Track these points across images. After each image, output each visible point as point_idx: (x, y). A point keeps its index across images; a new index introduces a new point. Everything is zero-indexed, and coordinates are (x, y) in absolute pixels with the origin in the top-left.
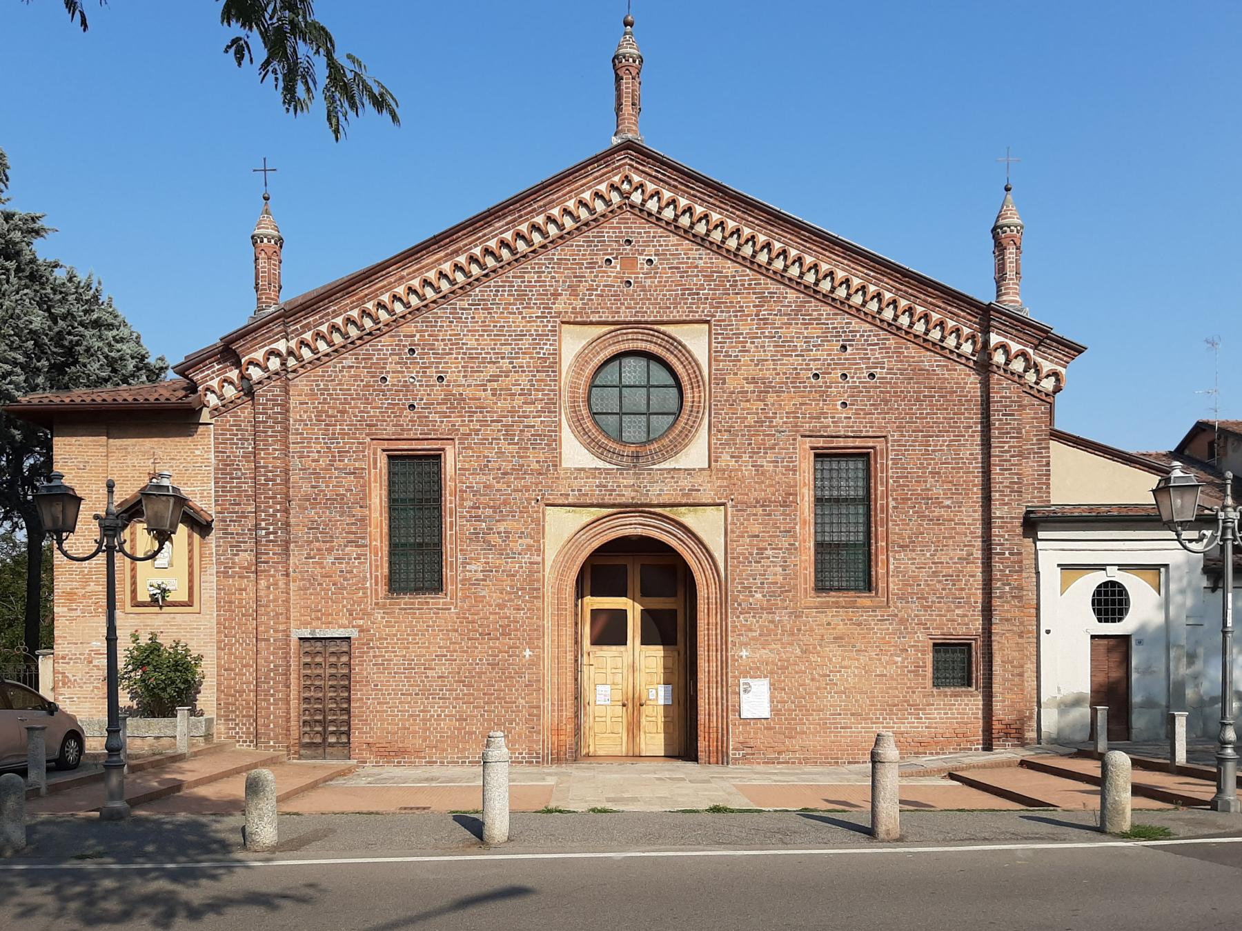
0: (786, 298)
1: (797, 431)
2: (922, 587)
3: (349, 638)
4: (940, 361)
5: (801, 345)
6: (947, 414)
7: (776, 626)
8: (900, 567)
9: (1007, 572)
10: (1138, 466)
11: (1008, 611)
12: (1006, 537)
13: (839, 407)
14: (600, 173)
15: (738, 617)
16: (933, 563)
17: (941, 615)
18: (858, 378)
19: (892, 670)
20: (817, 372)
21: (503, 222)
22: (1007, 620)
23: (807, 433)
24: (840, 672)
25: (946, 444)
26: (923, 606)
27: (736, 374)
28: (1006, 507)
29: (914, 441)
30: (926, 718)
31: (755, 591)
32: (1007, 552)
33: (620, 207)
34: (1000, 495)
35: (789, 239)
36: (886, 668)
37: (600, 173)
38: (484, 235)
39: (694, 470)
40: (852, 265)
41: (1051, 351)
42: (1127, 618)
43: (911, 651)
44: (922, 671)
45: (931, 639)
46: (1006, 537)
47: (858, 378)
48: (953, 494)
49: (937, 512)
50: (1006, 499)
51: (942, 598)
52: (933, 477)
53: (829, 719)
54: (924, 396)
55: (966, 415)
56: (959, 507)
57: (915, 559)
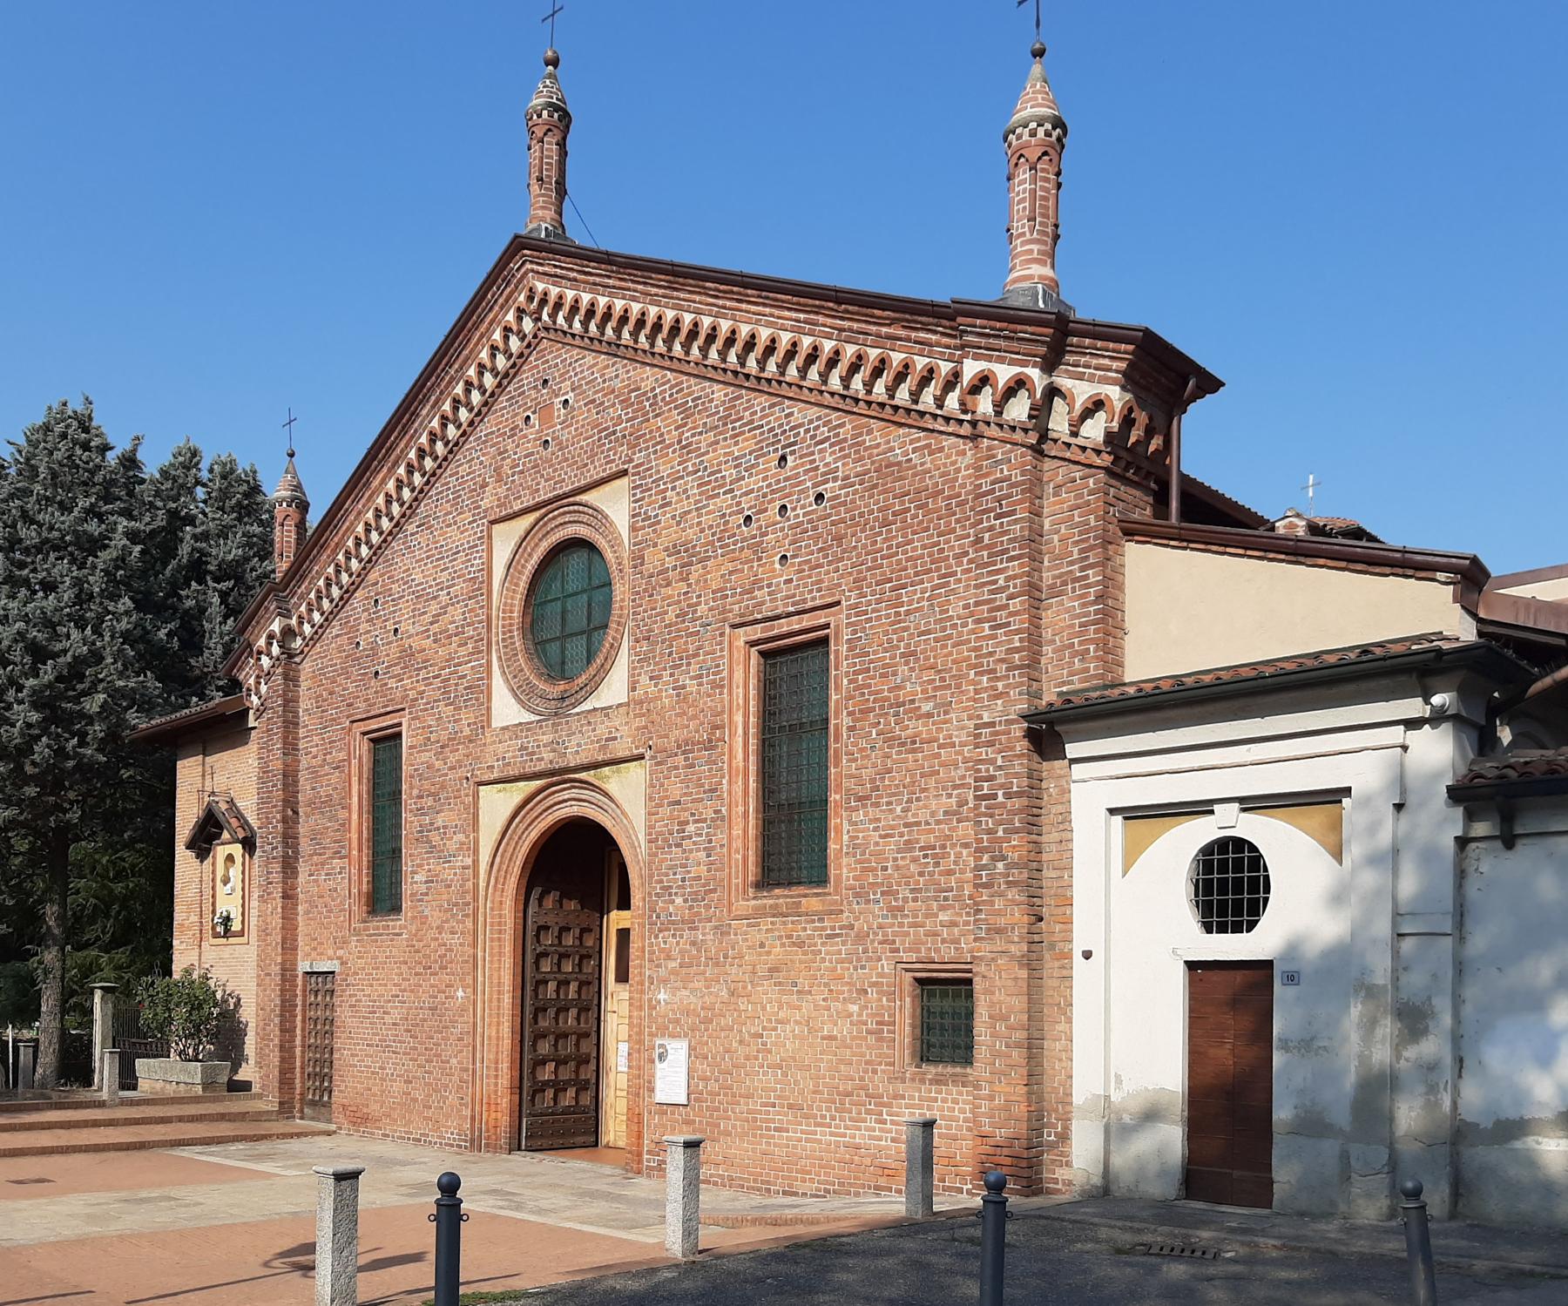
0: (711, 401)
1: (724, 620)
2: (890, 871)
3: (333, 972)
4: (919, 439)
5: (729, 473)
6: (929, 537)
7: (699, 951)
8: (858, 838)
9: (1000, 833)
10: (1321, 561)
11: (999, 913)
12: (999, 762)
13: (777, 566)
14: (504, 296)
15: (656, 937)
16: (906, 825)
17: (915, 925)
18: (803, 507)
19: (844, 1029)
20: (749, 513)
21: (428, 407)
22: (999, 931)
23: (738, 620)
24: (775, 1029)
25: (927, 595)
26: (891, 909)
27: (655, 545)
28: (1000, 702)
29: (878, 602)
30: (893, 1122)
31: (676, 894)
32: (1000, 793)
33: (535, 336)
34: (990, 680)
35: (700, 303)
36: (836, 1025)
37: (504, 296)
38: (416, 431)
39: (611, 707)
40: (776, 312)
41: (1087, 358)
42: (1265, 920)
43: (873, 994)
44: (889, 1032)
45: (907, 970)
46: (999, 762)
47: (803, 507)
48: (935, 689)
49: (915, 726)
50: (1000, 685)
51: (919, 891)
52: (907, 663)
53: (760, 1112)
54: (894, 514)
55: (959, 532)
56: (946, 713)
57: (878, 820)
